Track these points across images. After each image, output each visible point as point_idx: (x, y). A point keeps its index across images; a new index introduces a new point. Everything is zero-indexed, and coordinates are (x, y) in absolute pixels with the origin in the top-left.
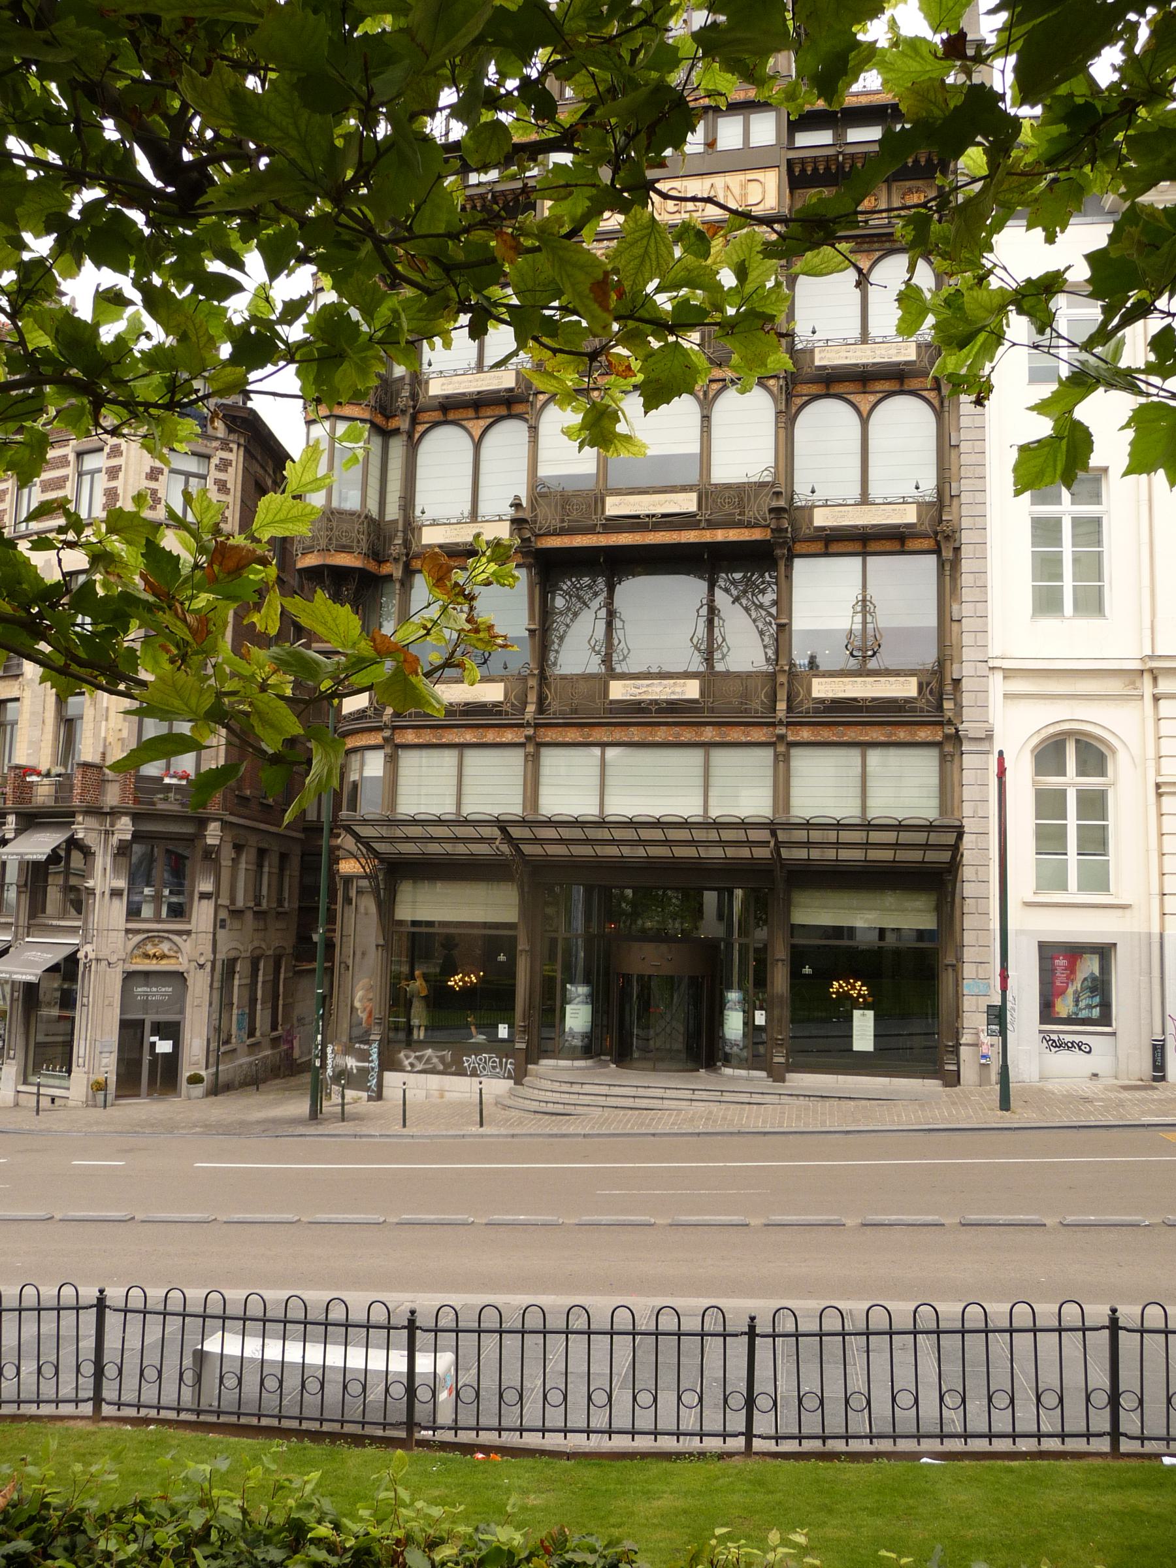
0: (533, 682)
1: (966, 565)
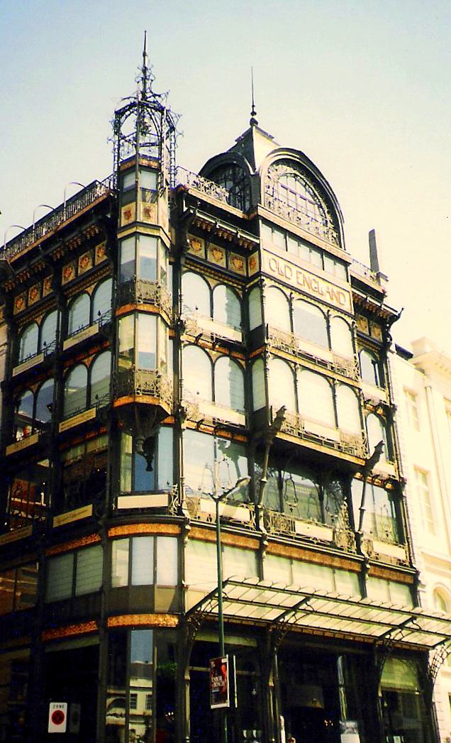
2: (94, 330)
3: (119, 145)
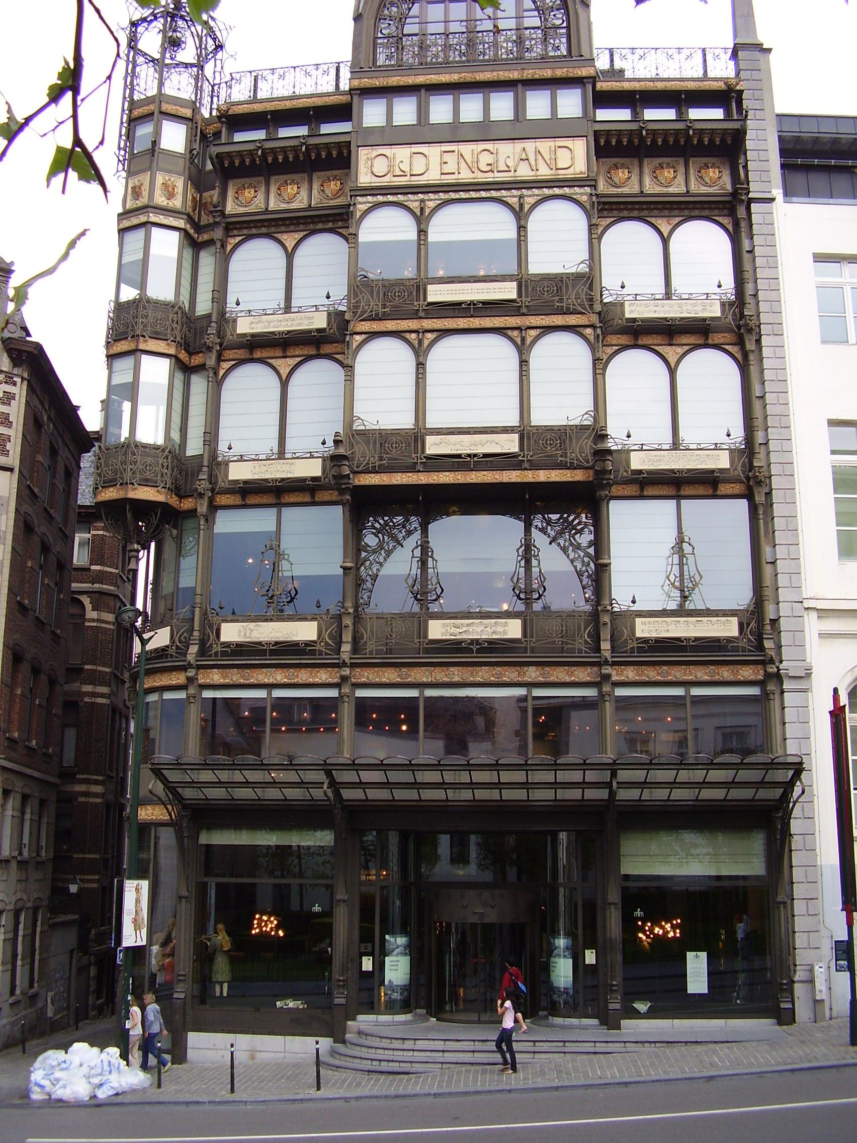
0: (348, 621)
1: (777, 510)
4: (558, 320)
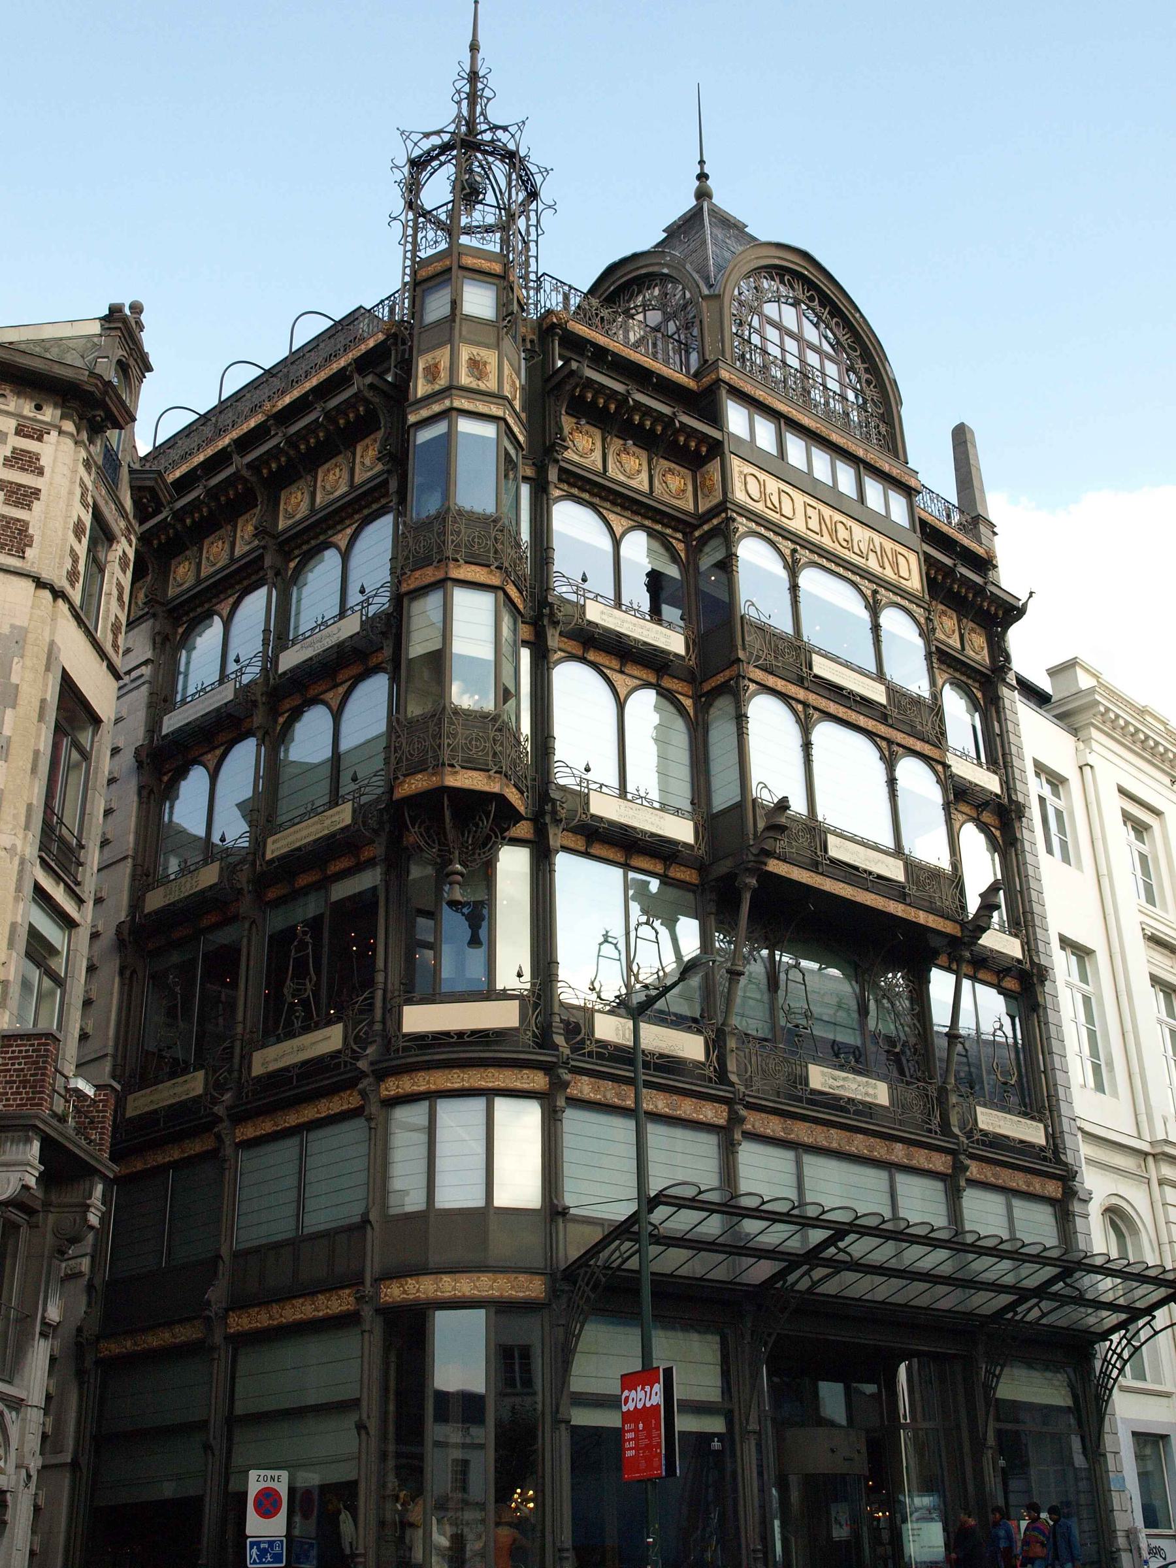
2: (351, 626)
3: (416, 229)
4: (919, 746)
